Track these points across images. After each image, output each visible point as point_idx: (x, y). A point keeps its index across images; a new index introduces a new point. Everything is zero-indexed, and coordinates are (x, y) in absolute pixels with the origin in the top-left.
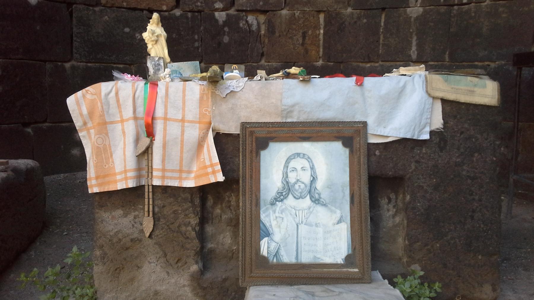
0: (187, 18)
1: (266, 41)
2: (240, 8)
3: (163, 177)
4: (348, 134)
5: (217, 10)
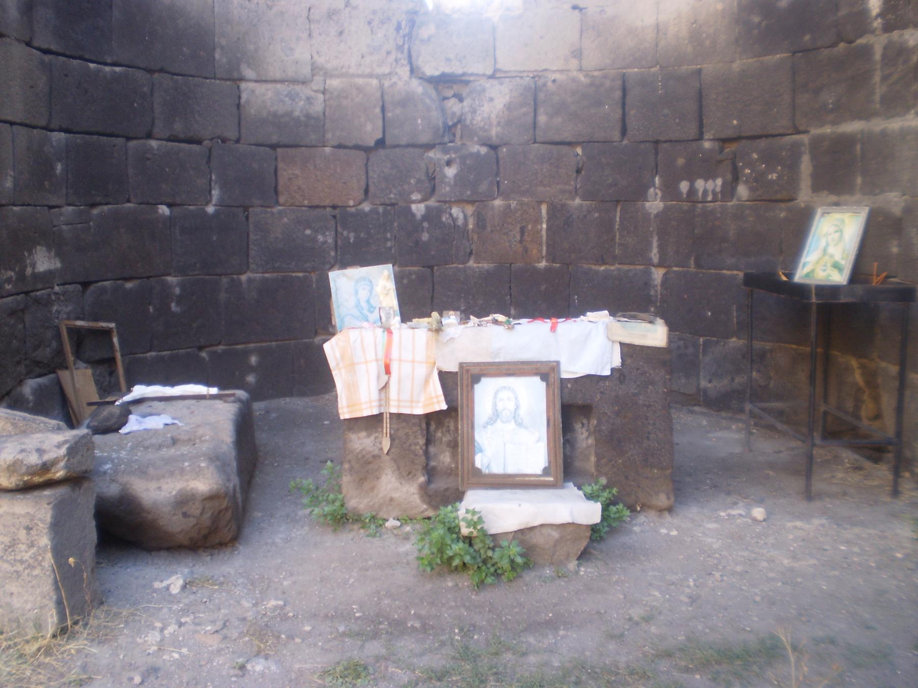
0: (378, 213)
1: (475, 237)
2: (442, 199)
3: (399, 406)
4: (546, 371)
5: (414, 202)
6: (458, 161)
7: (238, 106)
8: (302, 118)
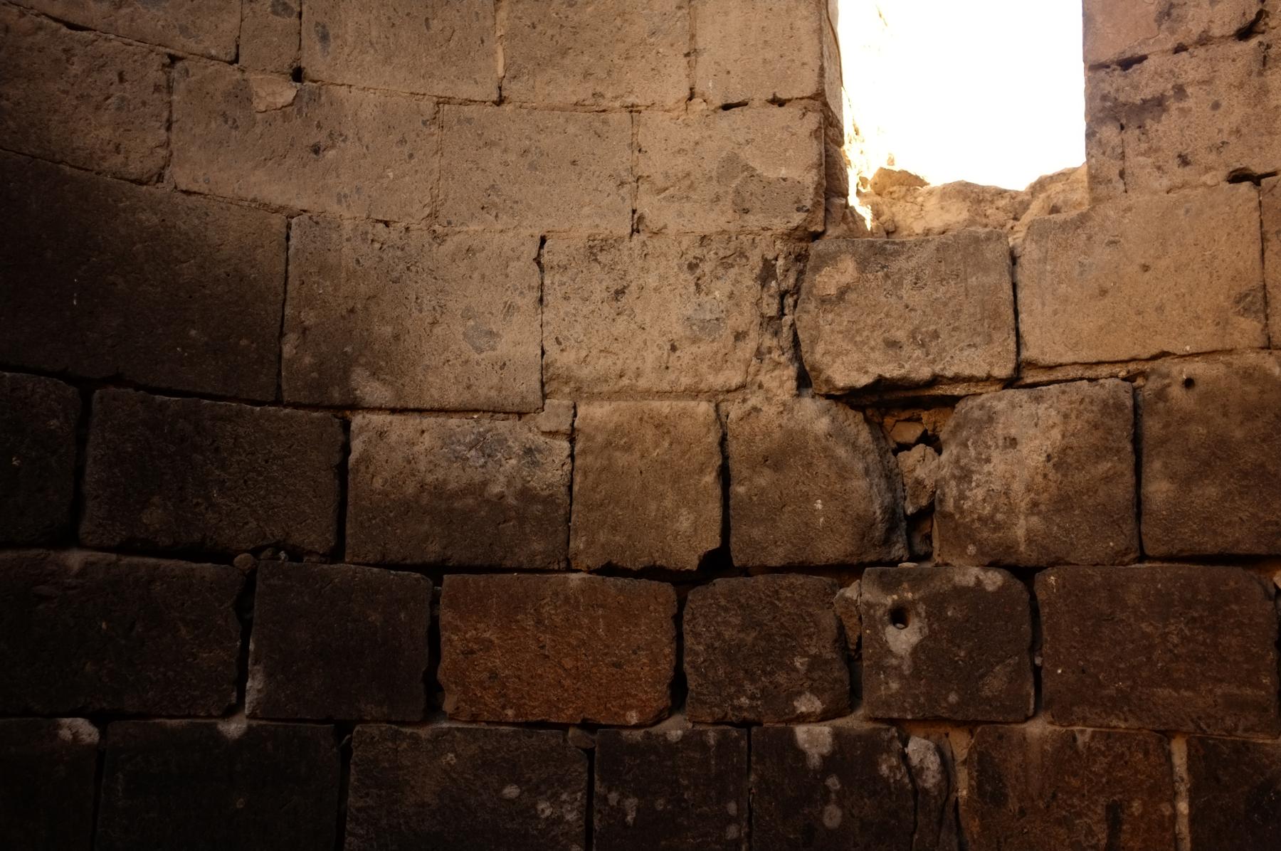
0: (704, 746)
2: (879, 714)
5: (803, 719)
6: (921, 608)
7: (342, 471)
8: (511, 501)
